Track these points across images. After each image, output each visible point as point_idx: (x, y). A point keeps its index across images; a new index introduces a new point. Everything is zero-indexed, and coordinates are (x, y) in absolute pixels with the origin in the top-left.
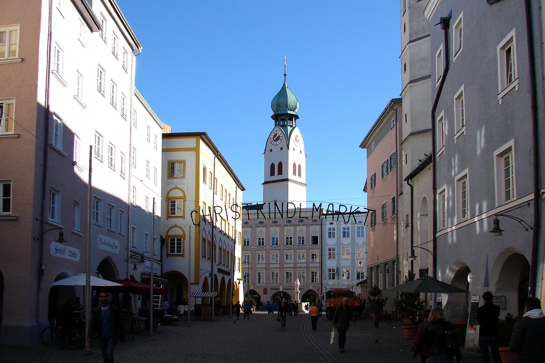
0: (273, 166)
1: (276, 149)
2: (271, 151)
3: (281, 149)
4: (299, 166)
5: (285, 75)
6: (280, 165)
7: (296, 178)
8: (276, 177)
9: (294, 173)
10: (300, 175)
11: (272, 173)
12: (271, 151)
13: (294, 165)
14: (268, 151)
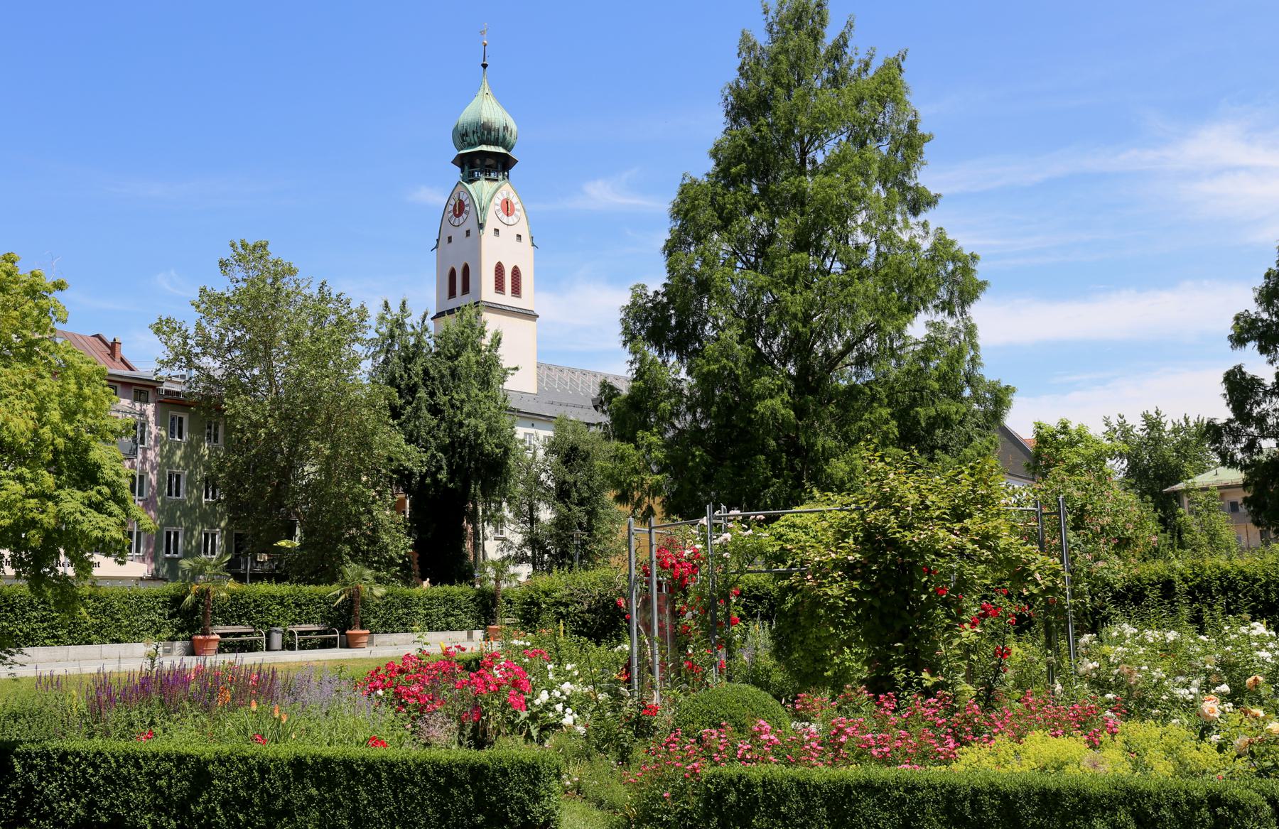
0: (453, 273)
1: (458, 234)
2: (450, 239)
3: (468, 233)
4: (516, 273)
5: (485, 66)
6: (466, 269)
7: (507, 299)
8: (460, 300)
9: (499, 287)
10: (516, 290)
11: (452, 294)
12: (450, 239)
13: (499, 269)
14: (444, 241)
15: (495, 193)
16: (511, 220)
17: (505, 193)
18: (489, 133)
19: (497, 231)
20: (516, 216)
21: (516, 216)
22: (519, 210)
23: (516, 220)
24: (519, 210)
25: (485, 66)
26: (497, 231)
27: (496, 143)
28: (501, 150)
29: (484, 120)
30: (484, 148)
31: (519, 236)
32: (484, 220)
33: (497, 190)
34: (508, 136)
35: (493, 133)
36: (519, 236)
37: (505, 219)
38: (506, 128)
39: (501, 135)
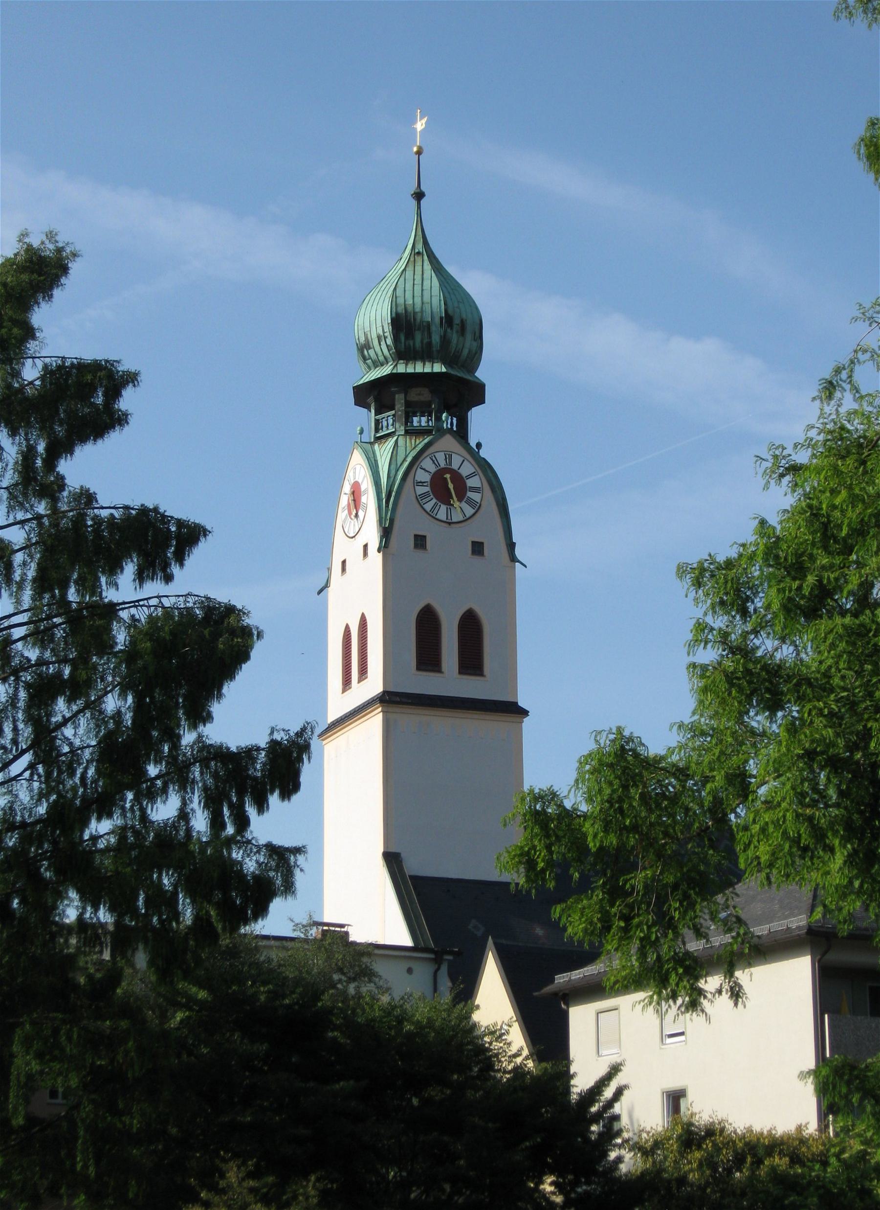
17: (441, 457)
18: (410, 335)
19: (420, 542)
20: (471, 502)
21: (471, 502)
24: (475, 490)
25: (419, 196)
26: (420, 542)
30: (401, 369)
31: (478, 548)
35: (418, 336)
39: (436, 339)
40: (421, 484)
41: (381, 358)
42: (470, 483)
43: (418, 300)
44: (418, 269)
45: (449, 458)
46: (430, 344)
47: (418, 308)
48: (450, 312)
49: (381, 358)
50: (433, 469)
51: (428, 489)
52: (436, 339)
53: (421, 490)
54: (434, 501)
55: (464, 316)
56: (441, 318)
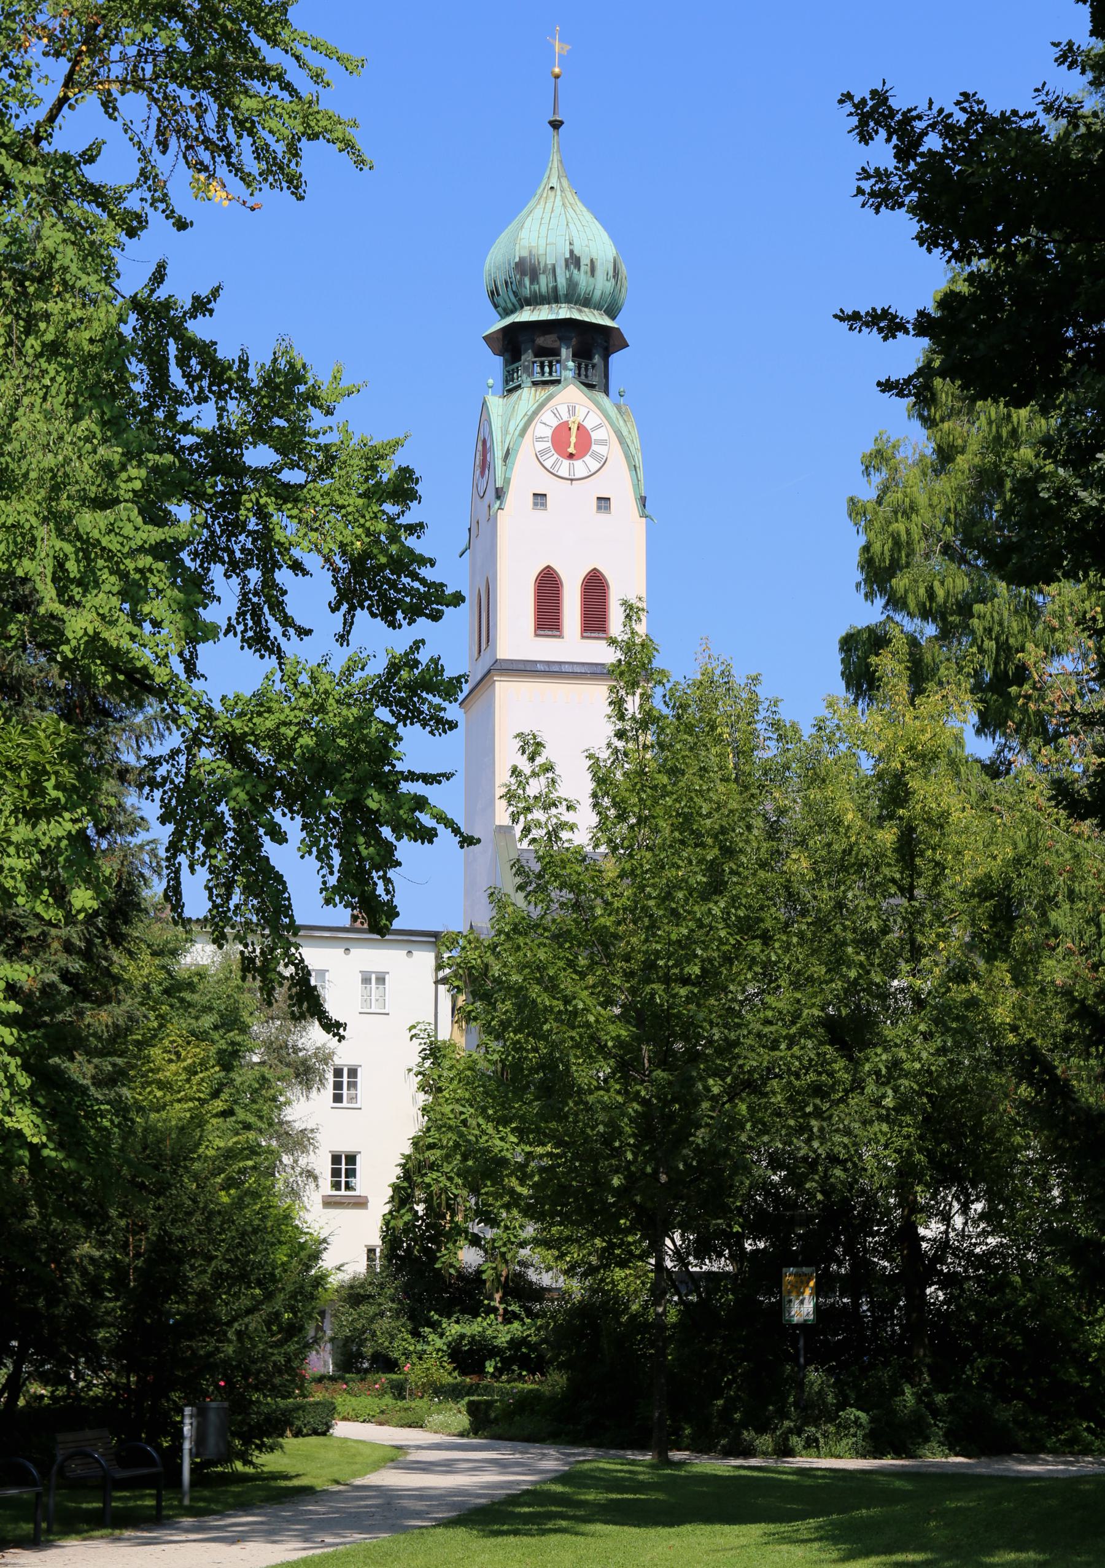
5: (556, 125)
15: (536, 413)
16: (580, 467)
18: (534, 279)
19: (540, 499)
20: (596, 456)
21: (596, 456)
22: (603, 442)
23: (594, 465)
24: (603, 442)
25: (556, 125)
27: (553, 298)
28: (563, 312)
29: (521, 251)
30: (526, 315)
31: (604, 502)
32: (507, 481)
33: (542, 406)
34: (582, 278)
35: (543, 279)
36: (604, 502)
37: (564, 467)
38: (574, 261)
39: (562, 282)
40: (540, 439)
41: (510, 306)
42: (595, 436)
43: (542, 242)
44: (549, 206)
45: (572, 410)
46: (555, 288)
47: (541, 251)
48: (576, 252)
49: (510, 306)
50: (555, 423)
51: (549, 444)
52: (562, 282)
53: (540, 446)
54: (556, 456)
55: (595, 256)
56: (566, 260)
